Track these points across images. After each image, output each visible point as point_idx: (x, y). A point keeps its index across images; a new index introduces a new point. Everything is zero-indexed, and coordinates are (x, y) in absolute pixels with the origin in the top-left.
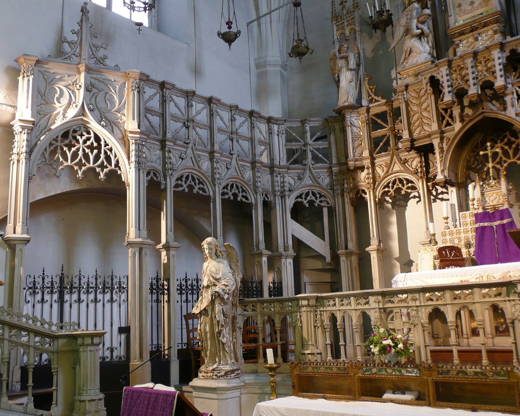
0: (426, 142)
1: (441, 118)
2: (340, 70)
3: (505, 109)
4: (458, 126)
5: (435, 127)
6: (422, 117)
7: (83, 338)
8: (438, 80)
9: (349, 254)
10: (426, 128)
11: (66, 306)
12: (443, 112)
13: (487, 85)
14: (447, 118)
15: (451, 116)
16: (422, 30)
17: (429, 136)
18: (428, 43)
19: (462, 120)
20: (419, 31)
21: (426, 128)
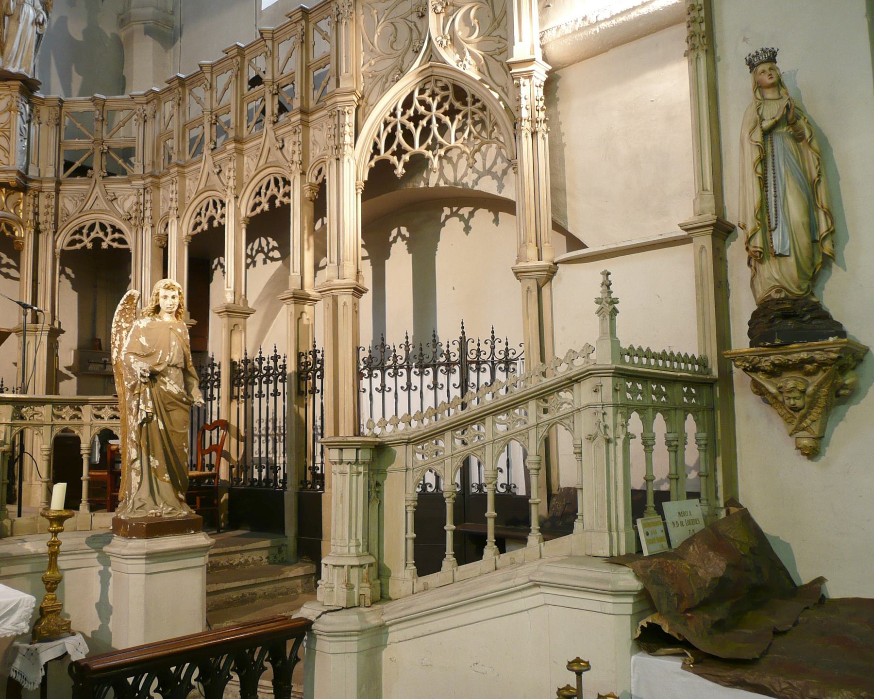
7: (341, 449)
11: (365, 398)
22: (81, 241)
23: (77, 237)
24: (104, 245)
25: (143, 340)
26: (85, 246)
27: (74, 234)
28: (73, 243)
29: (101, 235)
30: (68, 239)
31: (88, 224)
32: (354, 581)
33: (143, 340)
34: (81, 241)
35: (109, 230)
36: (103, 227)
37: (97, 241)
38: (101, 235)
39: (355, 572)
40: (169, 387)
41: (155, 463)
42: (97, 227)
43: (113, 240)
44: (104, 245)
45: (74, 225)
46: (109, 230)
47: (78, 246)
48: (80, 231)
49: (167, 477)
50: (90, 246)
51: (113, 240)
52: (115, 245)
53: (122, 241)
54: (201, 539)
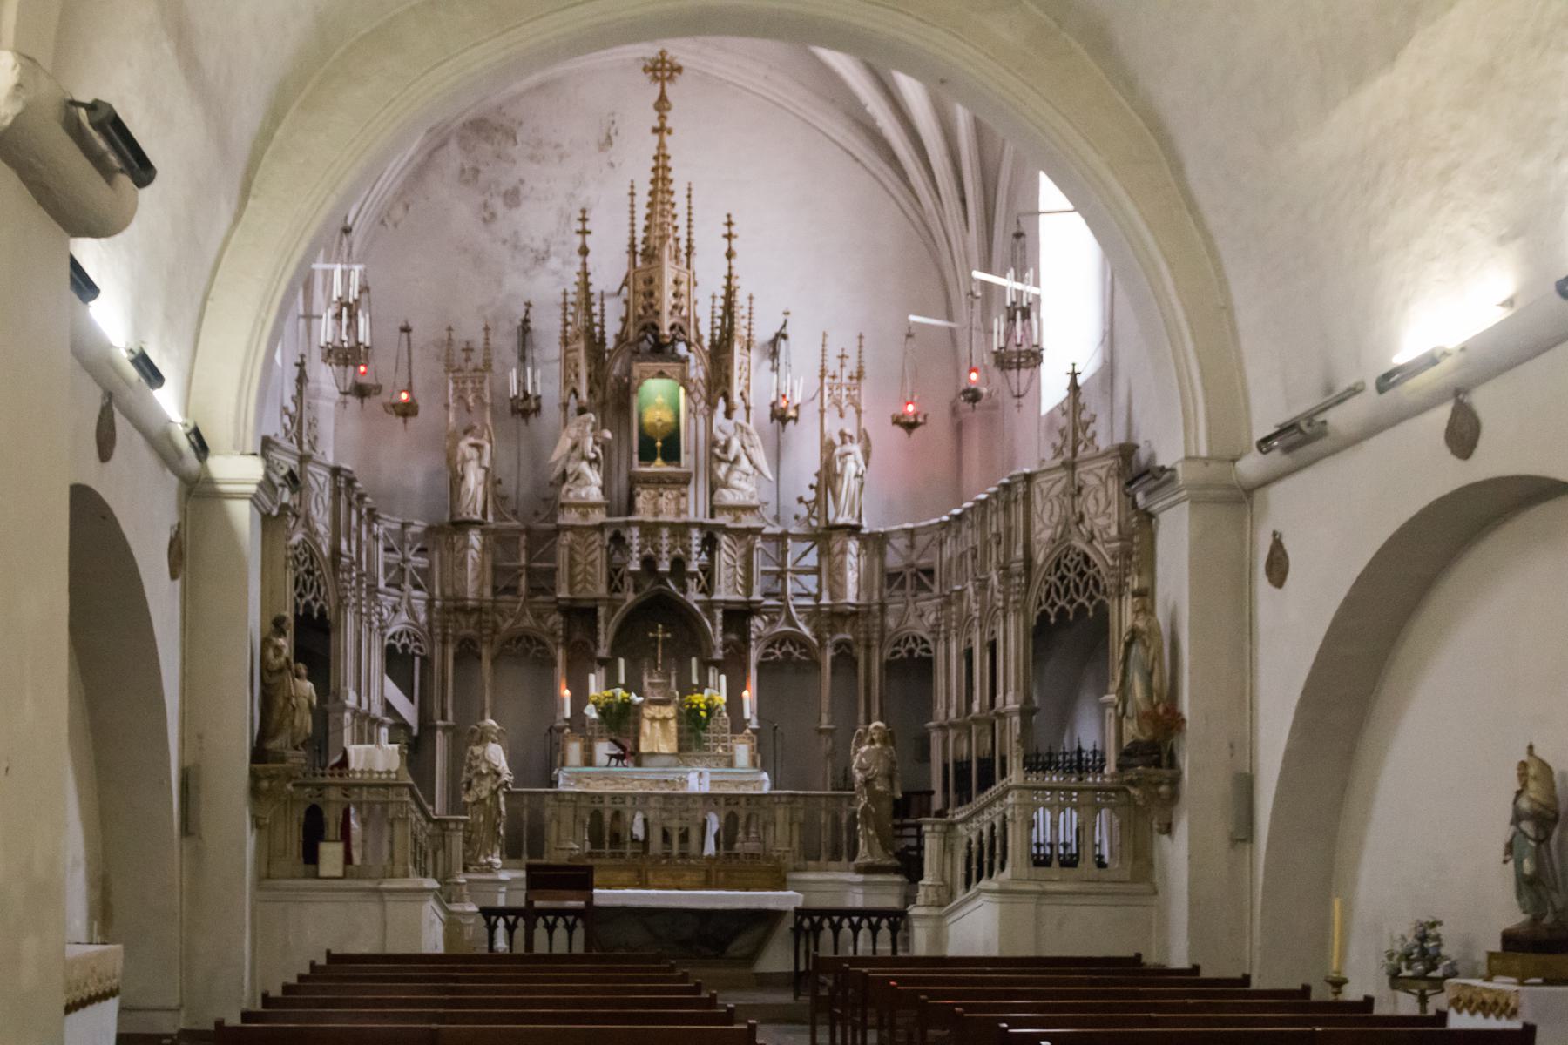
0: (590, 604)
1: (611, 580)
2: (465, 461)
3: (685, 591)
4: (631, 597)
5: (602, 590)
6: (585, 572)
8: (624, 539)
9: (445, 729)
10: (589, 586)
12: (613, 573)
13: (679, 564)
14: (616, 581)
15: (621, 581)
16: (596, 453)
17: (595, 600)
18: (598, 470)
19: (636, 591)
20: (593, 456)
21: (589, 586)
22: (899, 652)
23: (897, 648)
24: (916, 655)
25: (863, 760)
26: (902, 657)
27: (895, 646)
28: (894, 653)
29: (913, 646)
30: (892, 650)
31: (904, 637)
32: (930, 893)
33: (863, 760)
34: (899, 652)
35: (919, 641)
36: (915, 639)
37: (911, 651)
38: (913, 646)
39: (930, 889)
40: (878, 788)
41: (871, 832)
42: (911, 639)
43: (922, 650)
44: (916, 655)
45: (894, 639)
46: (919, 641)
47: (898, 656)
48: (898, 644)
49: (877, 841)
50: (906, 655)
51: (922, 650)
52: (924, 654)
53: (928, 651)
54: (898, 878)
